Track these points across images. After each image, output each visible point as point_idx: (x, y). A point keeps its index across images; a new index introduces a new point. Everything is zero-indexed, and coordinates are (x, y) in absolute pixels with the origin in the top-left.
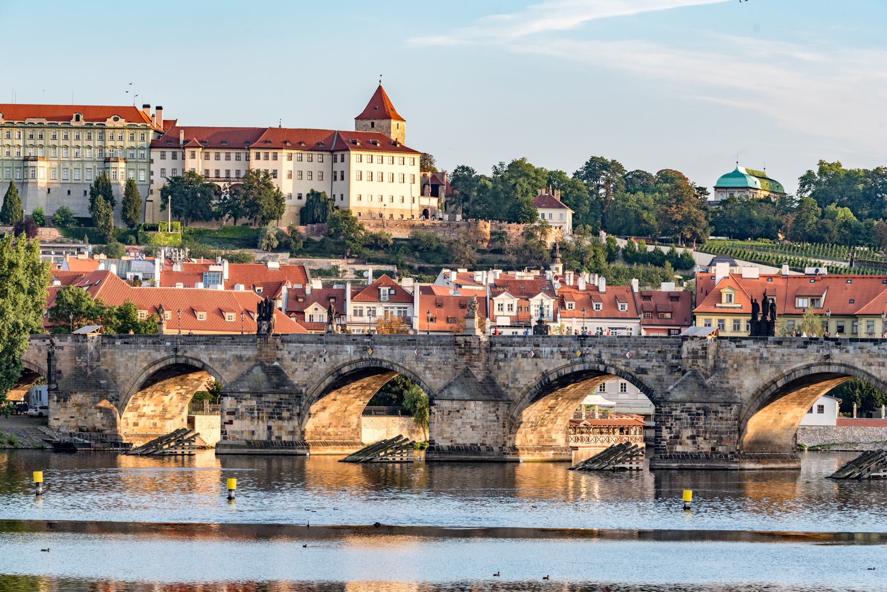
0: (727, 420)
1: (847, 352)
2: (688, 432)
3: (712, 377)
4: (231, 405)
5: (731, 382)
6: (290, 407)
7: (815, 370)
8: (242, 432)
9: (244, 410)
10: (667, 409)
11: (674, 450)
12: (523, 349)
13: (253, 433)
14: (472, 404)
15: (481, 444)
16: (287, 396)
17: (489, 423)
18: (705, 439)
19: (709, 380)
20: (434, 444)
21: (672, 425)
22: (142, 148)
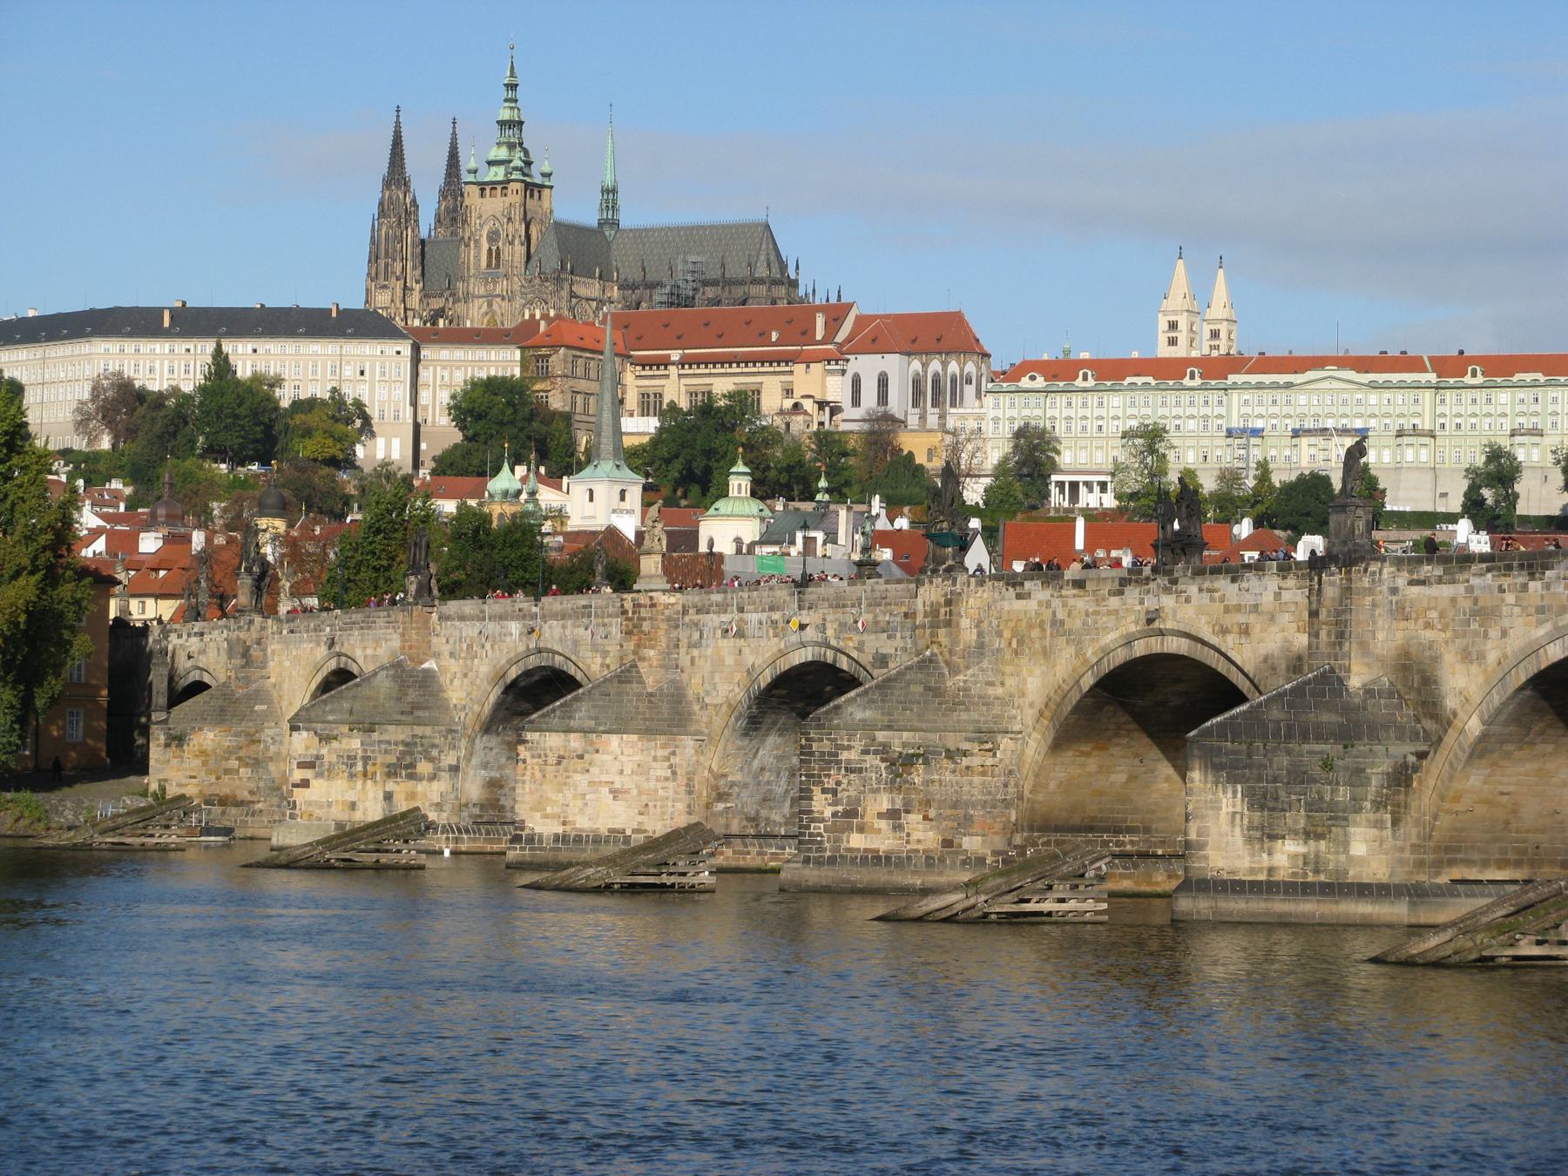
0: (984, 774)
1: (1188, 600)
2: (884, 802)
3: (970, 672)
4: (307, 748)
5: (1010, 682)
6: (435, 753)
7: (1140, 649)
8: (329, 804)
9: (334, 759)
10: (826, 746)
11: (844, 845)
12: (726, 618)
13: (353, 806)
14: (614, 740)
15: (634, 831)
16: (428, 731)
17: (652, 784)
18: (926, 818)
19: (961, 677)
20: (523, 829)
21: (838, 783)
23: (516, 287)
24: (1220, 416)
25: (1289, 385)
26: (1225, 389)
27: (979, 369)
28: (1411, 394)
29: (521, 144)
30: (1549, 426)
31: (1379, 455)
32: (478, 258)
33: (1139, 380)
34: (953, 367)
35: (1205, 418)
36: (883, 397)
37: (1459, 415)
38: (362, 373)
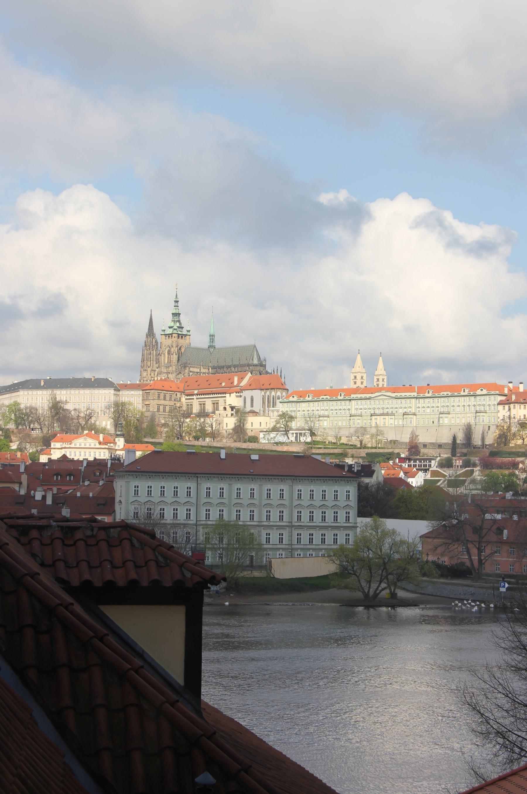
22: (494, 405)
23: (174, 369)
24: (349, 409)
25: (369, 399)
26: (350, 400)
27: (282, 394)
28: (408, 400)
29: (179, 321)
30: (452, 410)
31: (398, 422)
32: (164, 359)
33: (325, 397)
34: (273, 393)
35: (344, 409)
36: (252, 405)
37: (424, 407)
38: (99, 399)
